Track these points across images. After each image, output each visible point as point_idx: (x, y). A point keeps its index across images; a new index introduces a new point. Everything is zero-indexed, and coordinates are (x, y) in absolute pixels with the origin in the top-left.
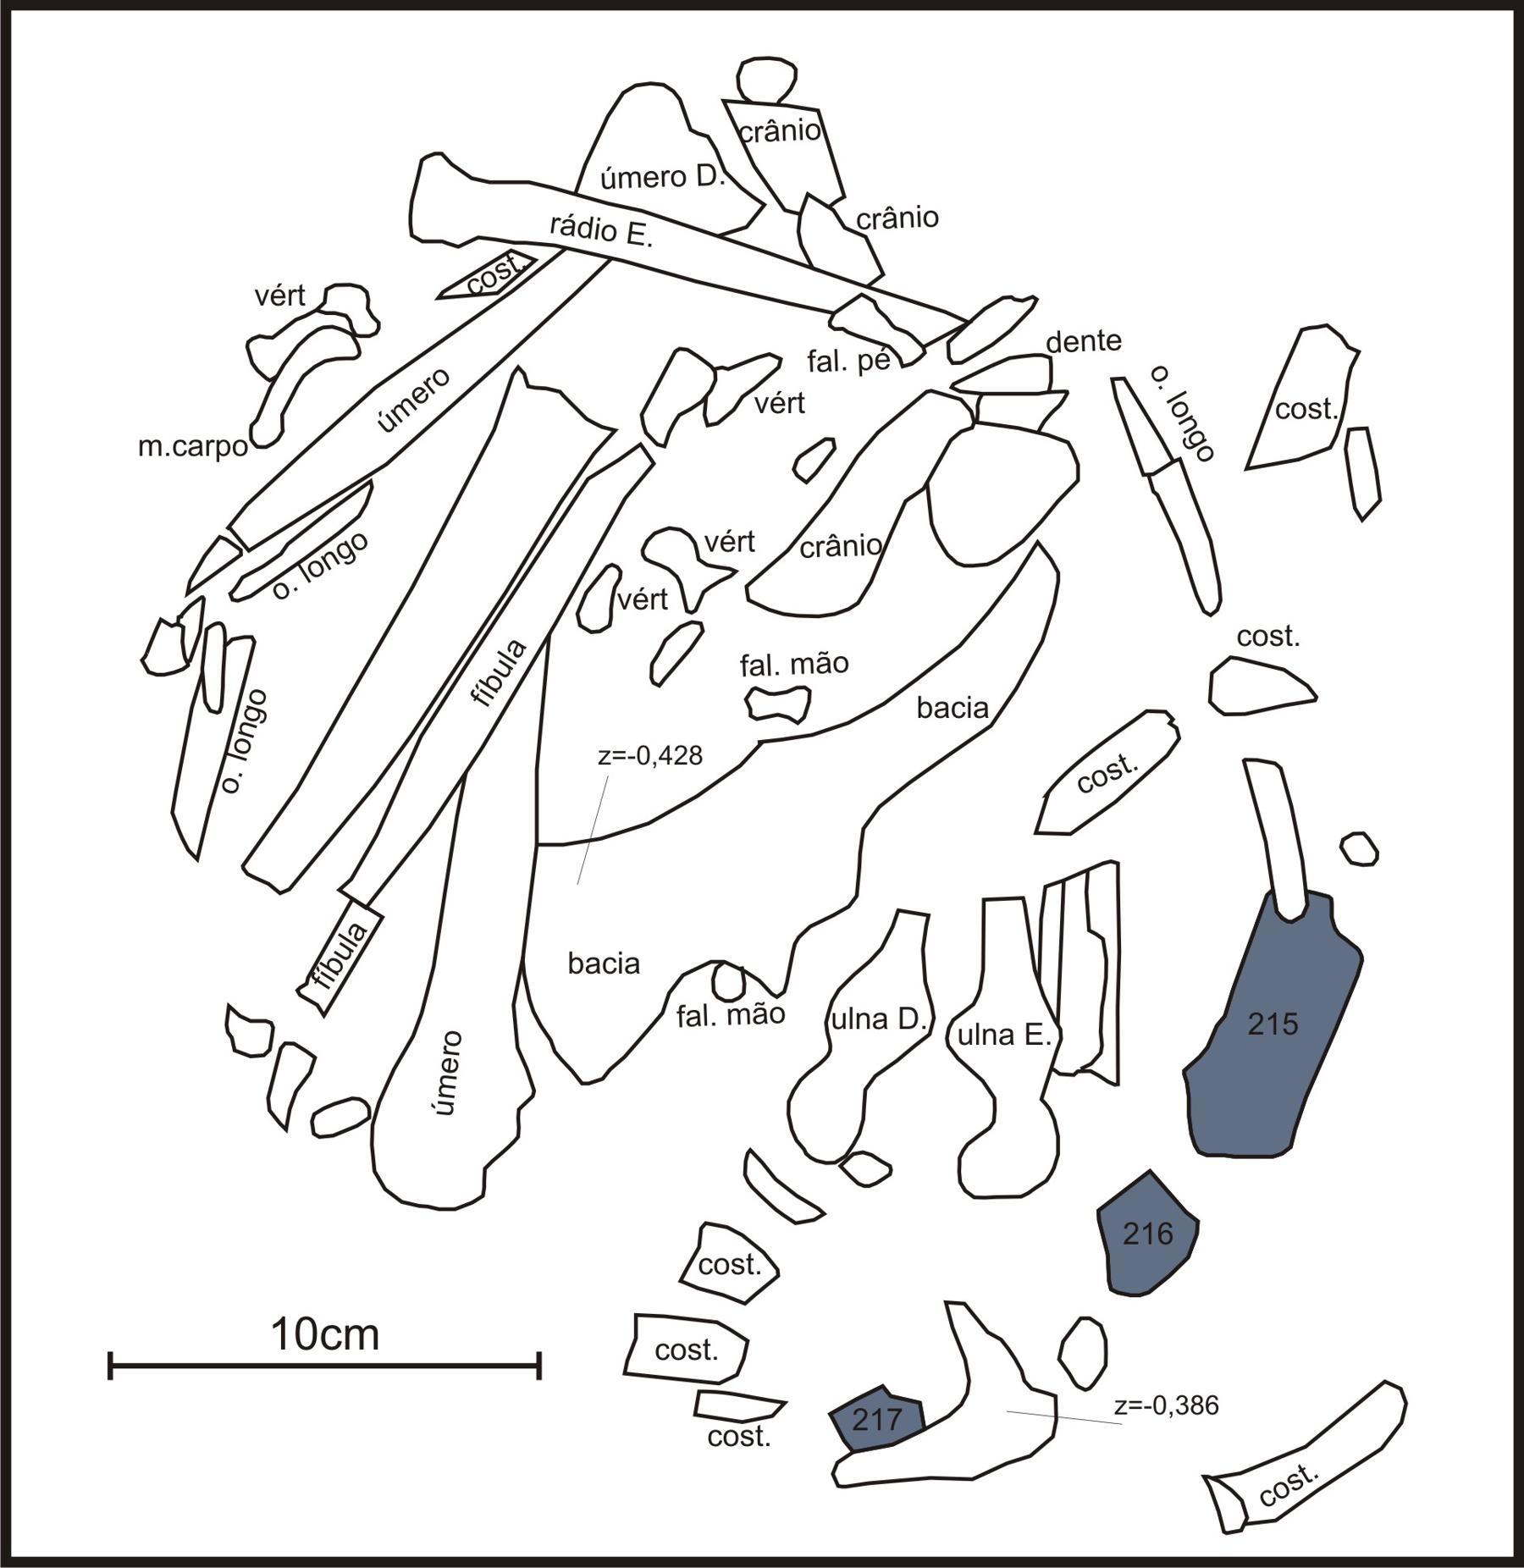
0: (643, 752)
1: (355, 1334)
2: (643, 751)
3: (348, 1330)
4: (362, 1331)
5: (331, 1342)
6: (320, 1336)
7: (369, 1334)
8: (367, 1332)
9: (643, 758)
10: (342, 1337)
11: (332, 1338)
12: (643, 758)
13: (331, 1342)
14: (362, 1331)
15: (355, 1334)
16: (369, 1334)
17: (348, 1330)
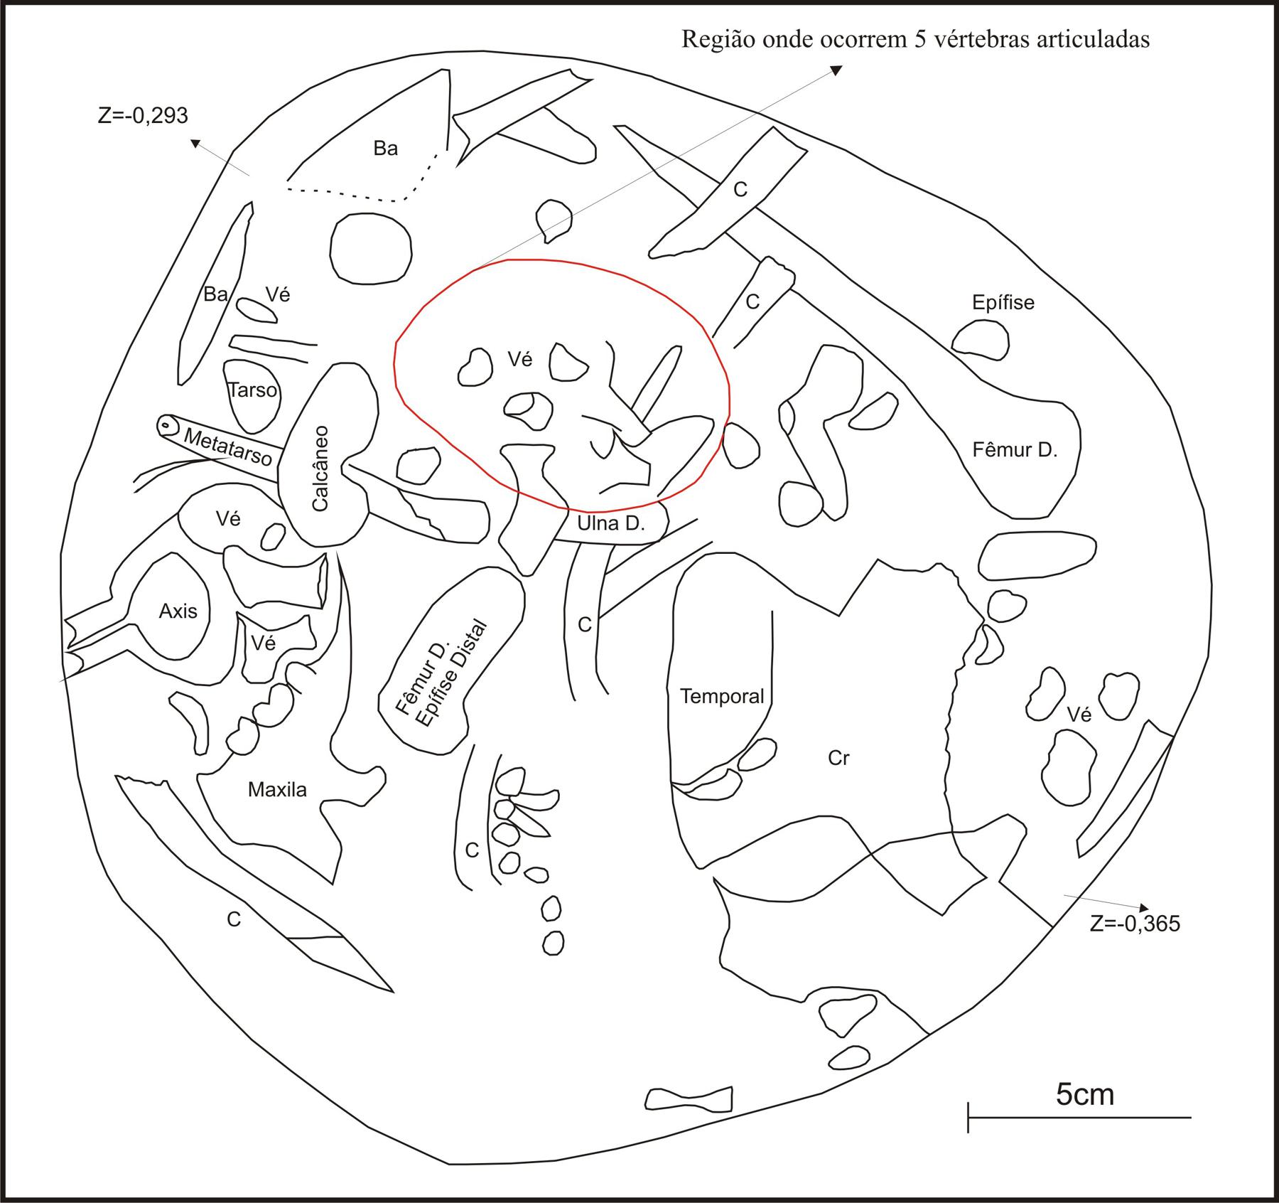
0: (138, 112)
1: (1097, 1094)
2: (139, 111)
3: (1093, 1092)
4: (1102, 1092)
5: (1082, 1101)
6: (1073, 1097)
7: (1107, 1094)
8: (1106, 1094)
9: (138, 118)
10: (1089, 1096)
11: (1082, 1097)
12: (138, 118)
13: (1082, 1101)
14: (1102, 1092)
15: (1097, 1094)
16: (1107, 1094)
17: (1093, 1092)
